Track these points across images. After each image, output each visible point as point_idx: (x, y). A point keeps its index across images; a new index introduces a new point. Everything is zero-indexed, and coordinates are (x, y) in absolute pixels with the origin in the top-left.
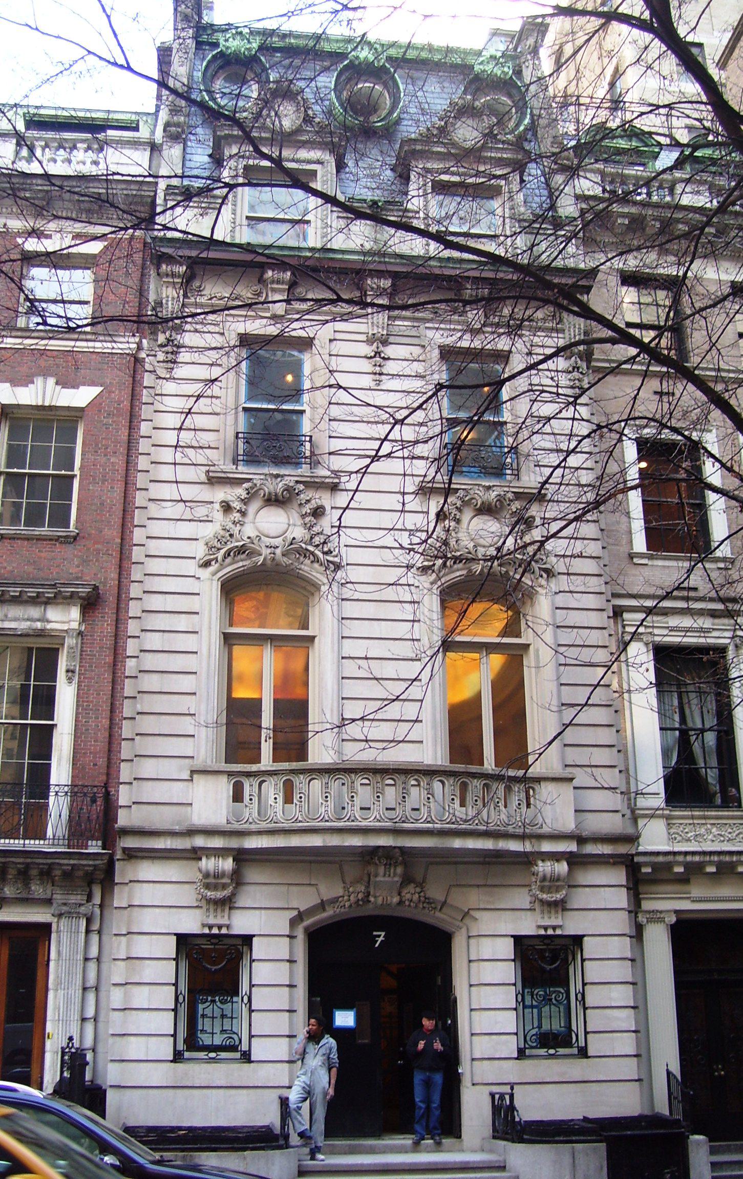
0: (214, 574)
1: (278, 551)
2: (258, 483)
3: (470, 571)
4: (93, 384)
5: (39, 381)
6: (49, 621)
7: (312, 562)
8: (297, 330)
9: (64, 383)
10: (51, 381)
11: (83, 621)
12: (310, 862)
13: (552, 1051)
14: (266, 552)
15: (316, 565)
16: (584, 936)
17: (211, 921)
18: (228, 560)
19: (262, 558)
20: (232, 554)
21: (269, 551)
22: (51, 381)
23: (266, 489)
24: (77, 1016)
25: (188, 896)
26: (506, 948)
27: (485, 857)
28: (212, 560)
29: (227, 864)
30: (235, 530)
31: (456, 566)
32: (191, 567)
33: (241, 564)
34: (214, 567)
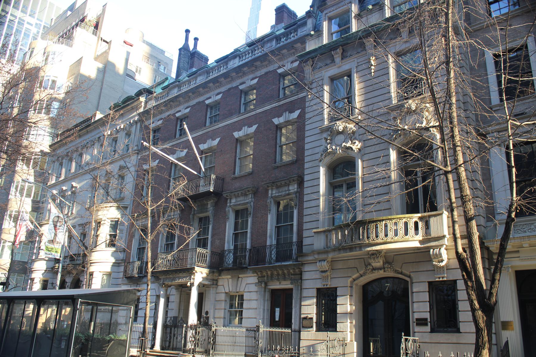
4: (299, 109)
5: (284, 114)
6: (290, 190)
8: (346, 67)
9: (291, 111)
10: (287, 112)
11: (299, 188)
12: (355, 259)
13: (446, 329)
16: (457, 280)
17: (324, 283)
22: (287, 112)
24: (298, 318)
25: (317, 275)
26: (426, 287)
27: (414, 250)
29: (325, 264)
32: (316, 163)
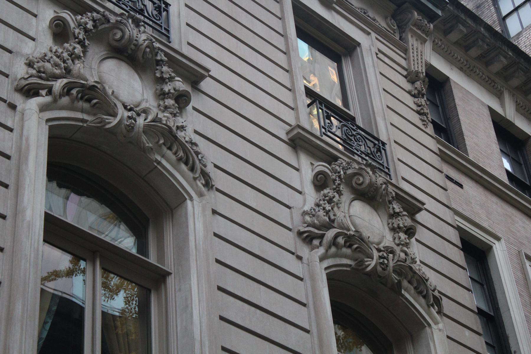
0: (43, 108)
1: (141, 121)
2: (113, 19)
3: (361, 263)
7: (180, 160)
14: (122, 113)
15: (183, 167)
18: (65, 100)
19: (114, 122)
20: (74, 92)
21: (127, 114)
23: (128, 33)
28: (43, 87)
30: (77, 67)
31: (344, 250)
33: (79, 115)
34: (43, 99)
